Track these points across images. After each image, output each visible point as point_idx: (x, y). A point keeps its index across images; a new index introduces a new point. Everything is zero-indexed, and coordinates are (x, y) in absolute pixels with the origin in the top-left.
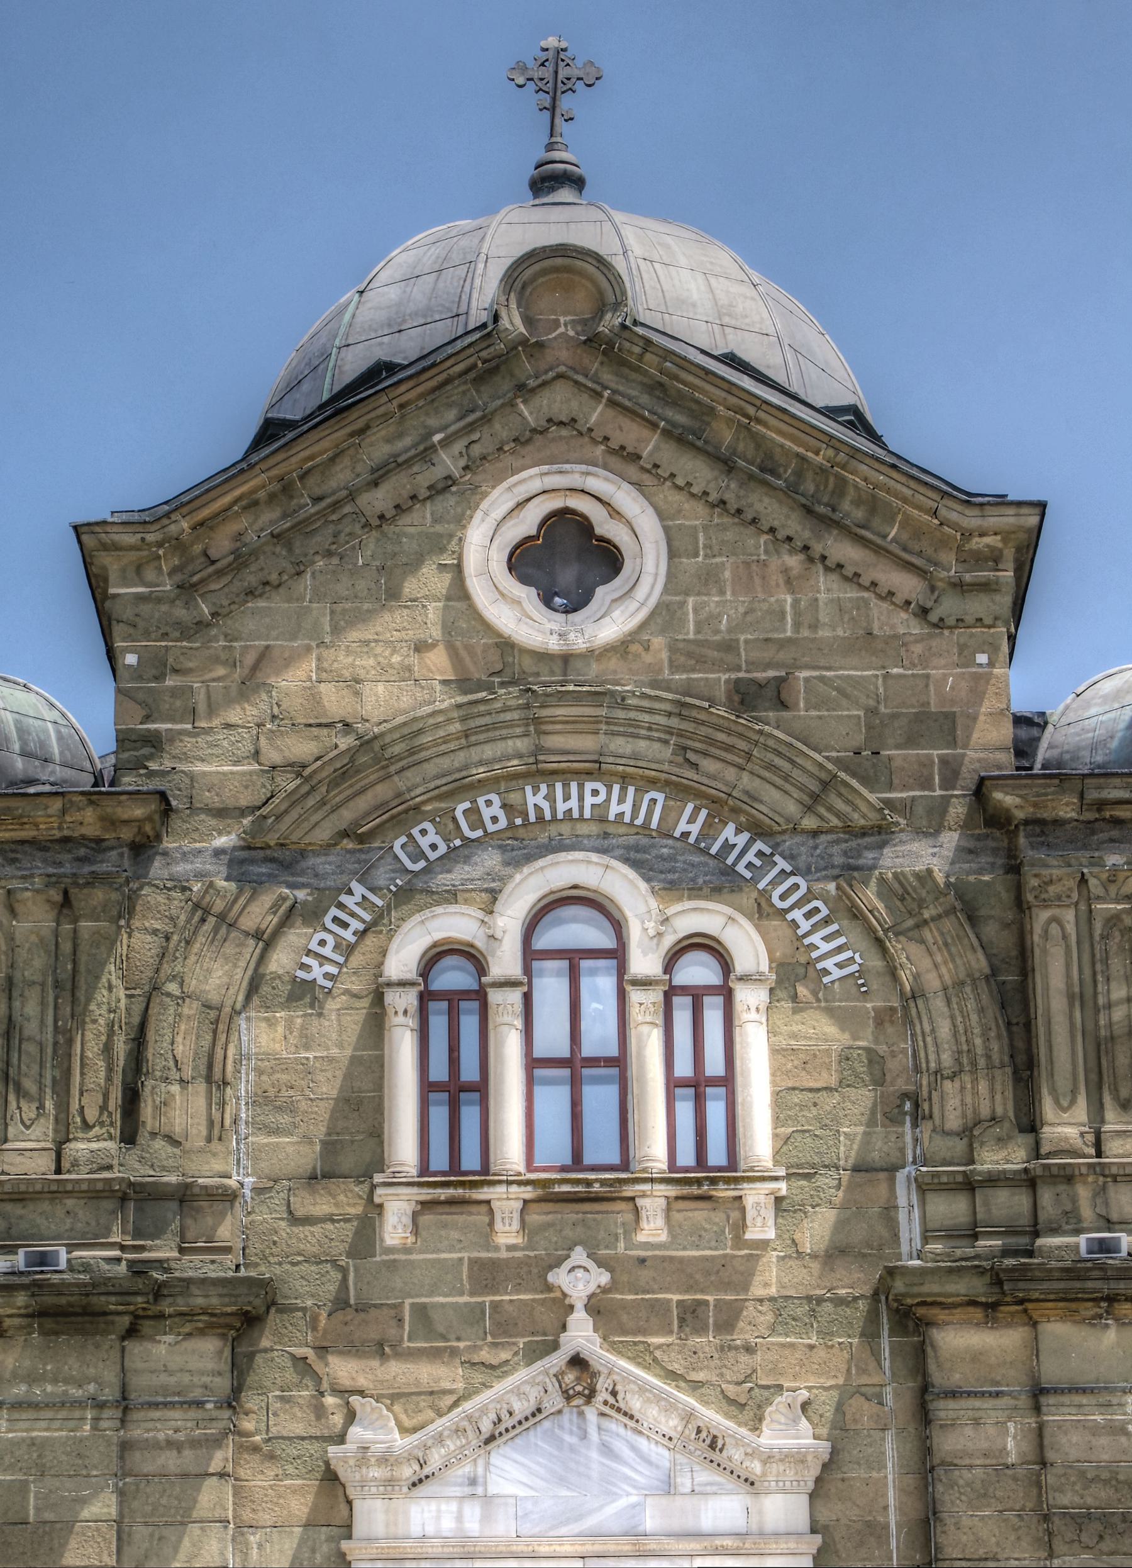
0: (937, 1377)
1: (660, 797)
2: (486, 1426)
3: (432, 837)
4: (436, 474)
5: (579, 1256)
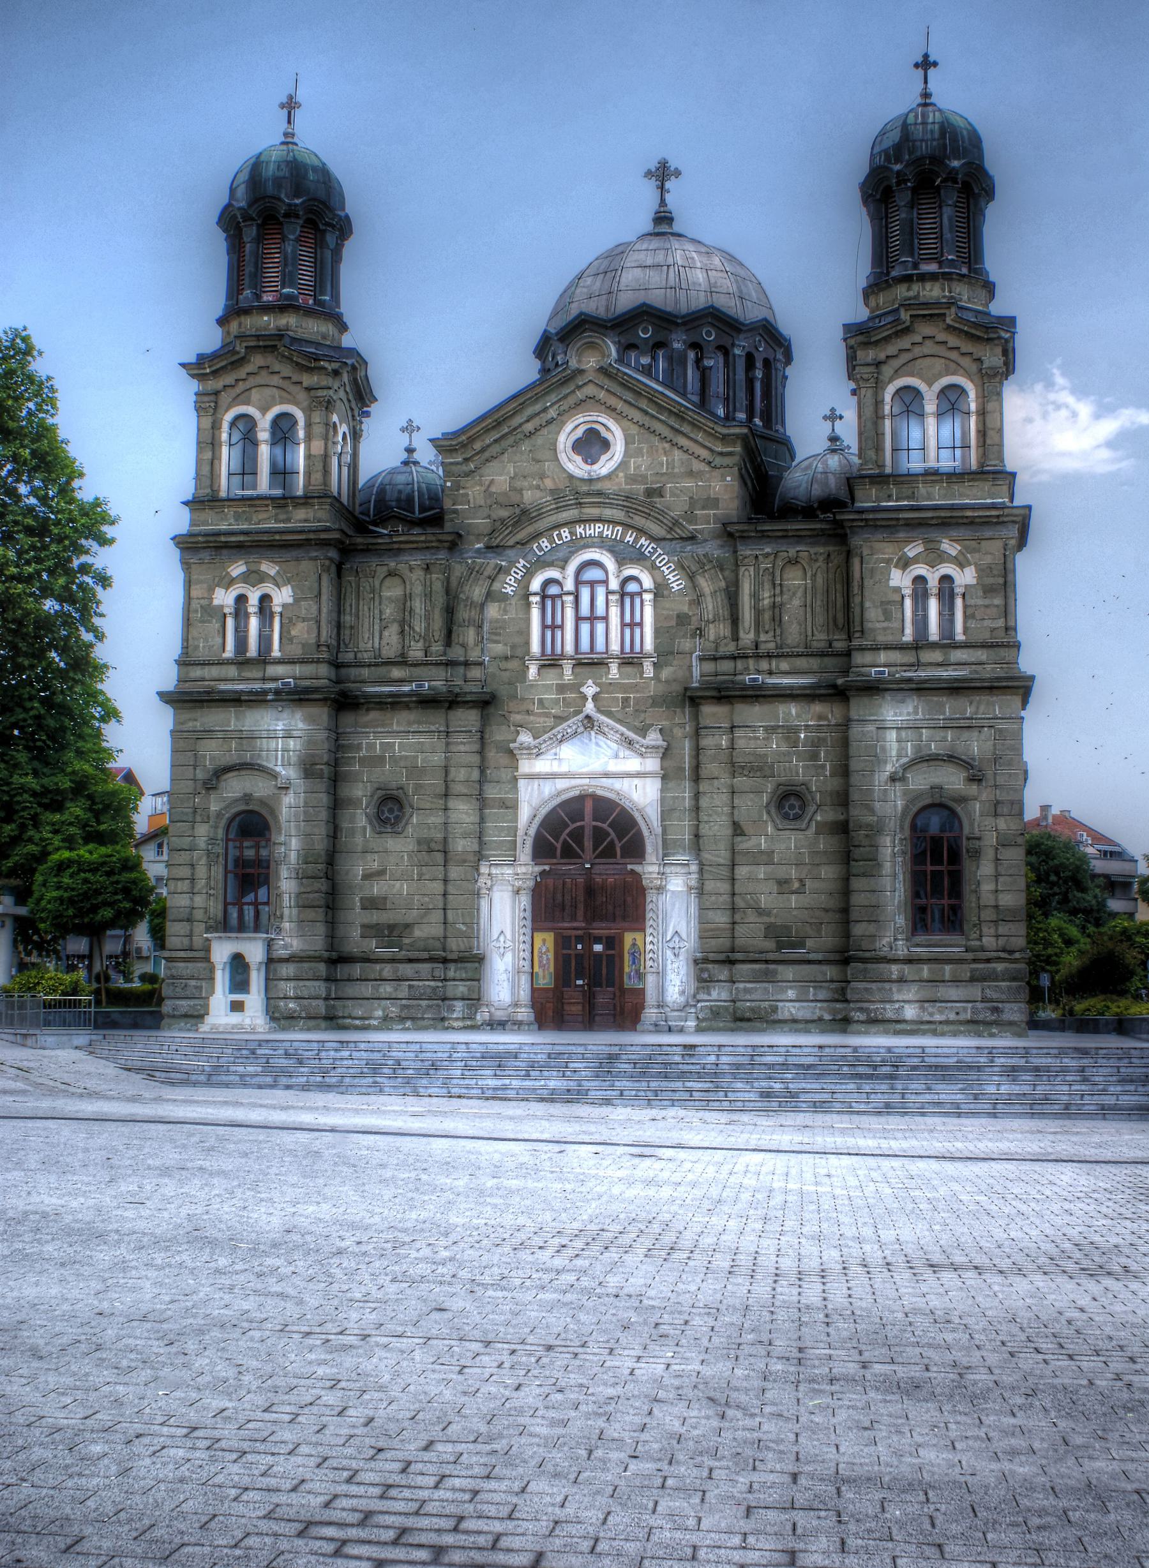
0: (703, 723)
1: (620, 529)
2: (559, 736)
3: (546, 544)
4: (549, 416)
5: (590, 682)
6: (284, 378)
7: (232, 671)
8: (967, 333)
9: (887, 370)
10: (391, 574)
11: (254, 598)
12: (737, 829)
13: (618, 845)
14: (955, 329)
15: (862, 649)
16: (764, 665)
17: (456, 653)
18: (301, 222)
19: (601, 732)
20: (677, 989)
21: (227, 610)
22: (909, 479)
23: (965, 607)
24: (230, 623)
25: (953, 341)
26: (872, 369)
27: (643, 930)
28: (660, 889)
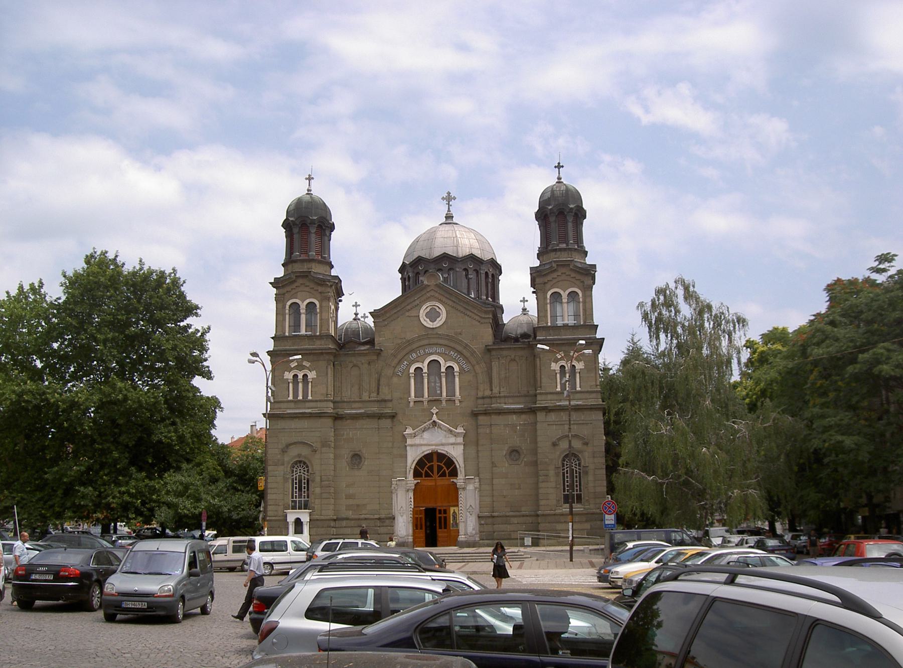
5: (434, 408)
6: (311, 288)
7: (292, 405)
8: (578, 272)
9: (548, 286)
10: (355, 366)
11: (300, 376)
12: (494, 465)
13: (447, 472)
14: (574, 270)
15: (540, 394)
16: (502, 400)
17: (381, 397)
18: (316, 226)
19: (440, 427)
21: (289, 381)
22: (555, 328)
23: (580, 377)
24: (291, 385)
25: (573, 275)
26: (542, 285)
27: (458, 506)
28: (464, 489)
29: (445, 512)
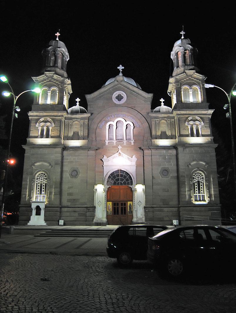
20: (140, 214)
27: (132, 201)
29: (125, 204)
